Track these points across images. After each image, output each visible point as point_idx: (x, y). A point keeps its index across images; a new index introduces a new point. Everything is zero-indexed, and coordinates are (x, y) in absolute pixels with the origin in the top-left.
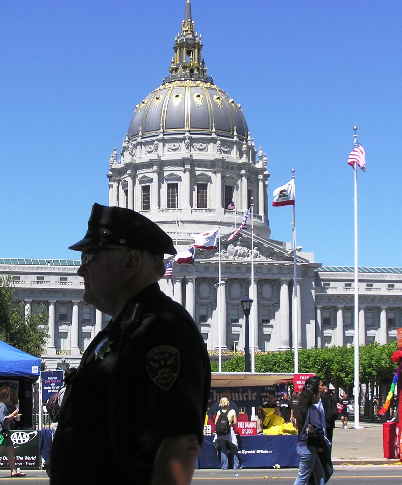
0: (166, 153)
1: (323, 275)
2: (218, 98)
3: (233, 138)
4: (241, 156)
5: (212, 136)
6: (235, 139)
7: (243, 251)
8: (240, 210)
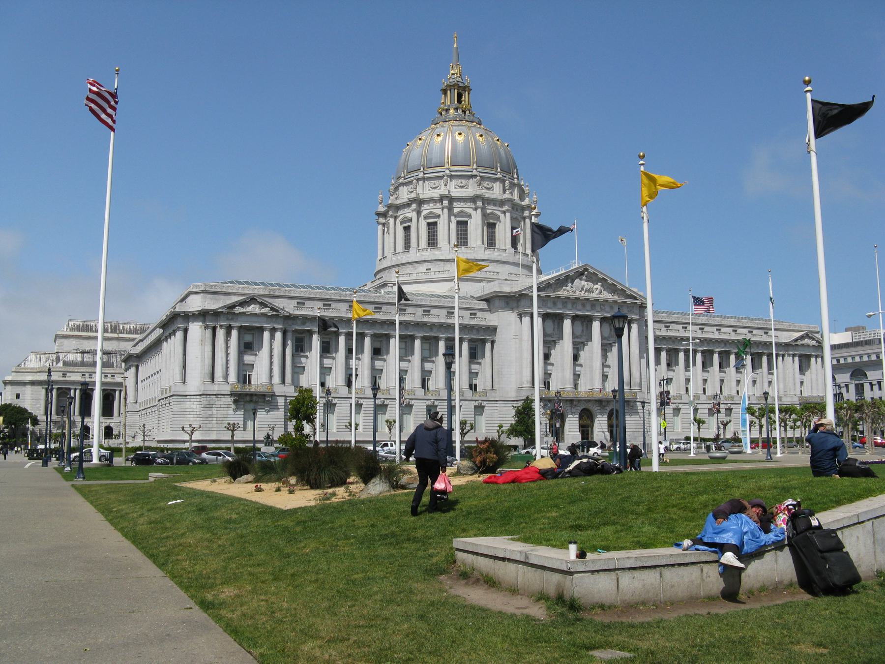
0: (425, 191)
2: (481, 136)
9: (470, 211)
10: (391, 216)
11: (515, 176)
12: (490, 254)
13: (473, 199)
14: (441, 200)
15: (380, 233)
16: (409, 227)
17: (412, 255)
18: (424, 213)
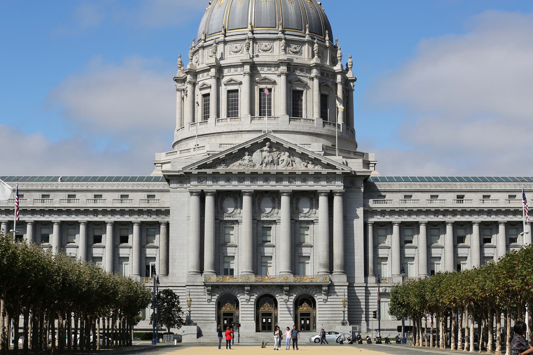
1: (381, 186)
3: (305, 37)
4: (313, 56)
5: (278, 35)
6: (307, 38)
7: (271, 159)
8: (311, 118)
9: (273, 77)
10: (189, 82)
11: (327, 38)
12: (297, 125)
13: (277, 65)
15: (178, 100)
16: (208, 95)
17: (211, 126)
18: (224, 80)
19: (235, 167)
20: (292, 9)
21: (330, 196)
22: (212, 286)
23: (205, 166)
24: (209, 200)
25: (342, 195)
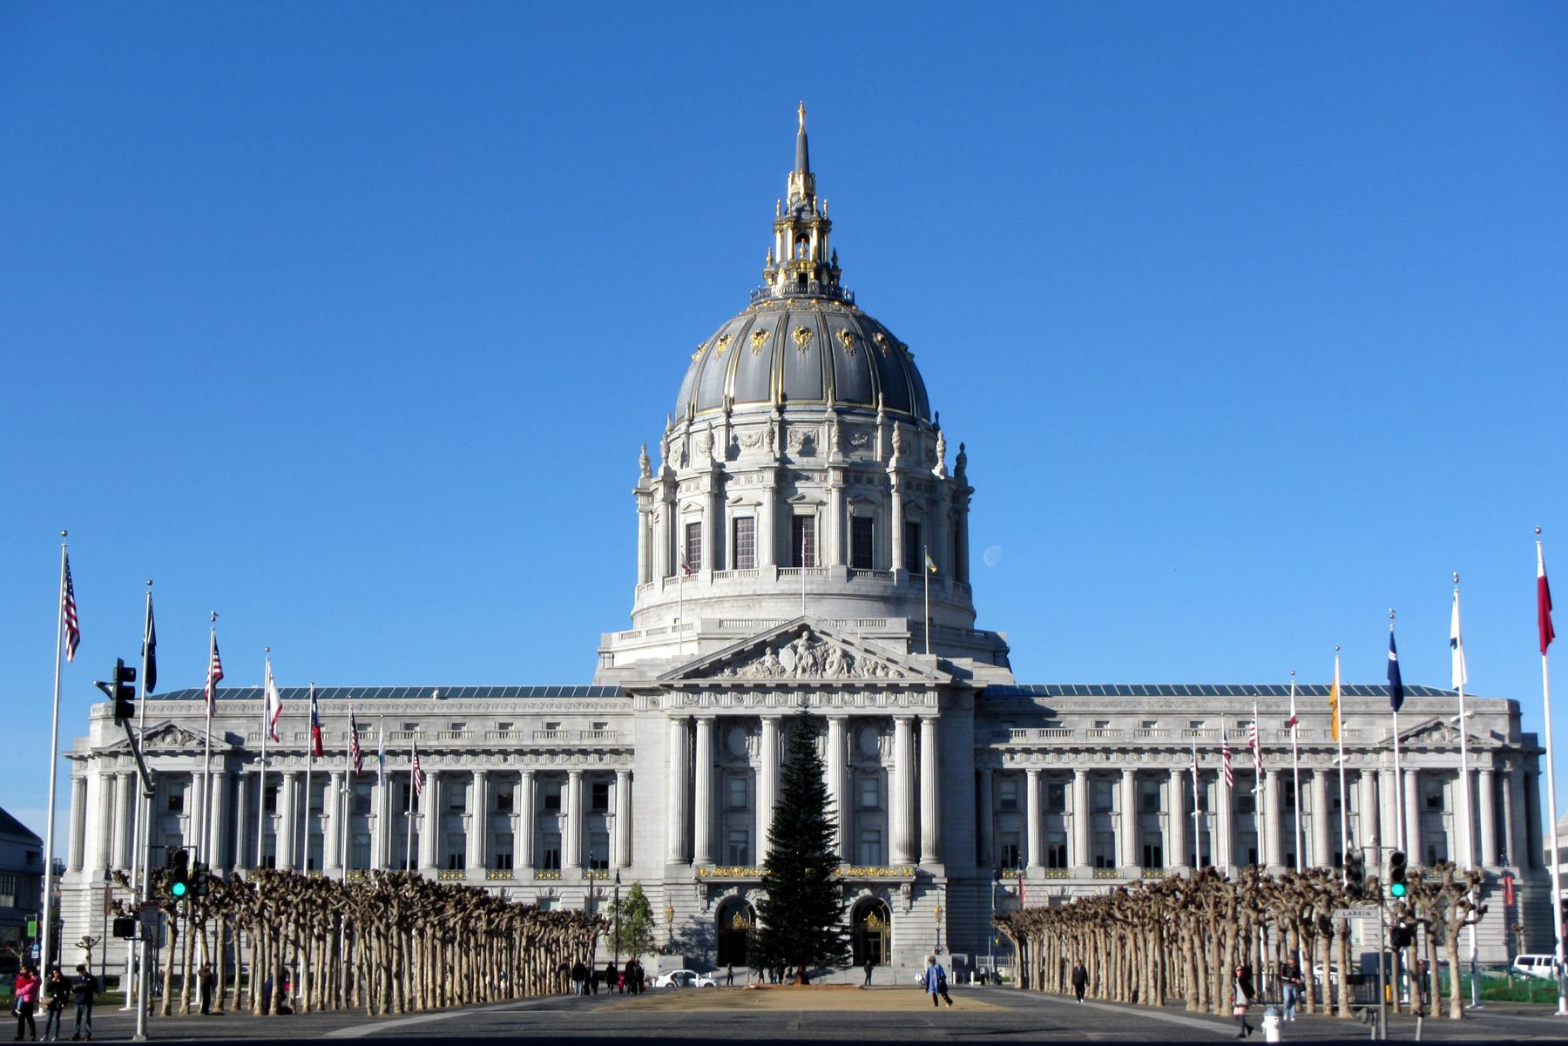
14: (763, 469)
19: (751, 673)
20: (850, 362)
21: (915, 725)
22: (710, 885)
23: (697, 673)
24: (702, 731)
25: (938, 724)
